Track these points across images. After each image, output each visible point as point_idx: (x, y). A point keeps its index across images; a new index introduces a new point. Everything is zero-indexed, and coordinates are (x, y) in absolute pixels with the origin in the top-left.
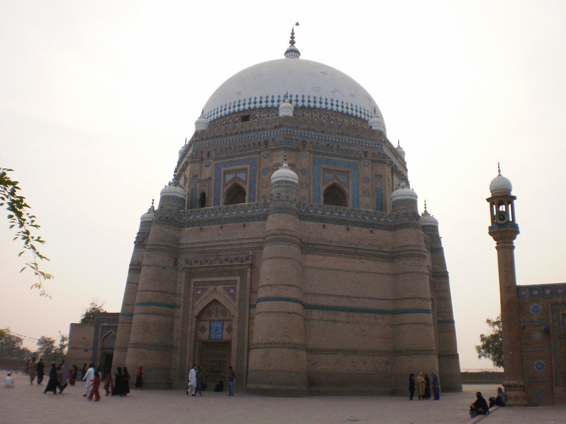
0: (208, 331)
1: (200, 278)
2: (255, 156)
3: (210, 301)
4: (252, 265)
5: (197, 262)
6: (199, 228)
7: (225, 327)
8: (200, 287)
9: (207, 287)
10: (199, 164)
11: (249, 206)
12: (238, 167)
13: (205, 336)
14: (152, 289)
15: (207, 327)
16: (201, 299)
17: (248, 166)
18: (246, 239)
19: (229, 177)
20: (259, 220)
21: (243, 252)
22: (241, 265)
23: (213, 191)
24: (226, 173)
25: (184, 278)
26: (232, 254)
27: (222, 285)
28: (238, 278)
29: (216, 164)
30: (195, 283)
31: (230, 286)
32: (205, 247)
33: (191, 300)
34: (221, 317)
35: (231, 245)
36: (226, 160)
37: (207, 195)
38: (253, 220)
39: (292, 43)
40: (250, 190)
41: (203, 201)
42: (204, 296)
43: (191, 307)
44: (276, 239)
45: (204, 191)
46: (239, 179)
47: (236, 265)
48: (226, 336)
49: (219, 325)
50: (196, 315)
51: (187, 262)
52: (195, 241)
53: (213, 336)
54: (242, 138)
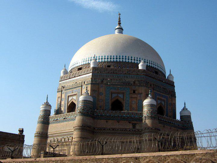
2: (168, 96)
17: (165, 99)
39: (120, 24)
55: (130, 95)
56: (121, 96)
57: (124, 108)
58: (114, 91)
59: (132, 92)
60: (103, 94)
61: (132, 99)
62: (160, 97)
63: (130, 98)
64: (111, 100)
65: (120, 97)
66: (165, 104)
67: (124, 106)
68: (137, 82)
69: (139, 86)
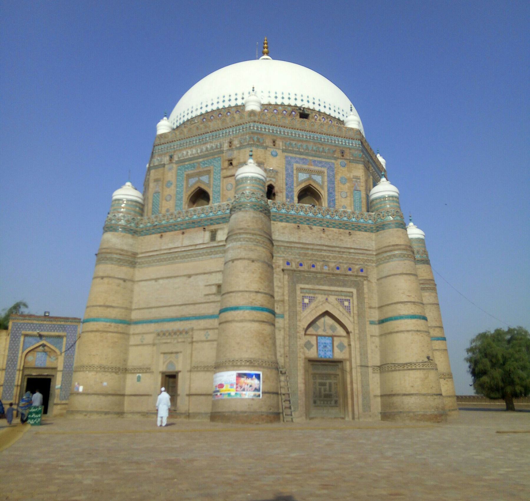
0: (315, 347)
1: (308, 284)
2: (333, 161)
3: (321, 313)
4: (367, 277)
5: (301, 265)
6: (295, 225)
7: (336, 344)
8: (307, 295)
9: (316, 296)
10: (263, 150)
11: (353, 213)
12: (312, 168)
13: (313, 353)
14: (261, 291)
15: (314, 342)
16: (308, 310)
18: (355, 249)
19: (303, 176)
20: (366, 231)
21: (353, 262)
22: (356, 276)
23: (284, 186)
24: (300, 170)
25: (286, 283)
26: (340, 263)
27: (335, 295)
28: (354, 291)
29: (286, 157)
30: (301, 289)
31: (344, 298)
32: (308, 249)
33: (298, 309)
34: (330, 332)
35: (339, 252)
36: (298, 156)
37: (276, 189)
38: (360, 230)
40: (328, 195)
41: (270, 192)
42: (313, 305)
43: (298, 318)
44: (408, 255)
45: (273, 184)
46: (314, 181)
47: (351, 275)
48: (338, 355)
49: (328, 341)
50: (305, 327)
51: (288, 264)
52: (292, 240)
53: (322, 354)
54: (313, 137)
55: (222, 173)
56: (205, 179)
57: (211, 201)
58: (192, 172)
59: (226, 164)
60: (171, 184)
61: (225, 180)
62: (306, 167)
63: (222, 179)
64: (187, 191)
65: (204, 183)
66: (323, 182)
67: (211, 198)
68: (236, 143)
69: (239, 148)
